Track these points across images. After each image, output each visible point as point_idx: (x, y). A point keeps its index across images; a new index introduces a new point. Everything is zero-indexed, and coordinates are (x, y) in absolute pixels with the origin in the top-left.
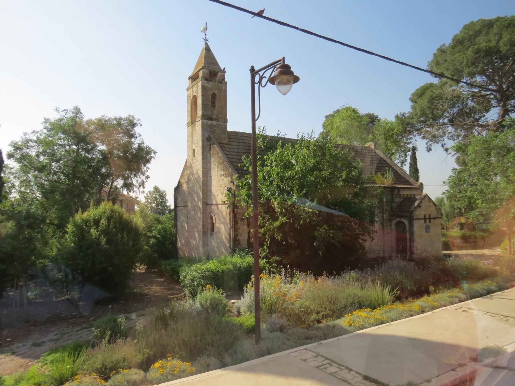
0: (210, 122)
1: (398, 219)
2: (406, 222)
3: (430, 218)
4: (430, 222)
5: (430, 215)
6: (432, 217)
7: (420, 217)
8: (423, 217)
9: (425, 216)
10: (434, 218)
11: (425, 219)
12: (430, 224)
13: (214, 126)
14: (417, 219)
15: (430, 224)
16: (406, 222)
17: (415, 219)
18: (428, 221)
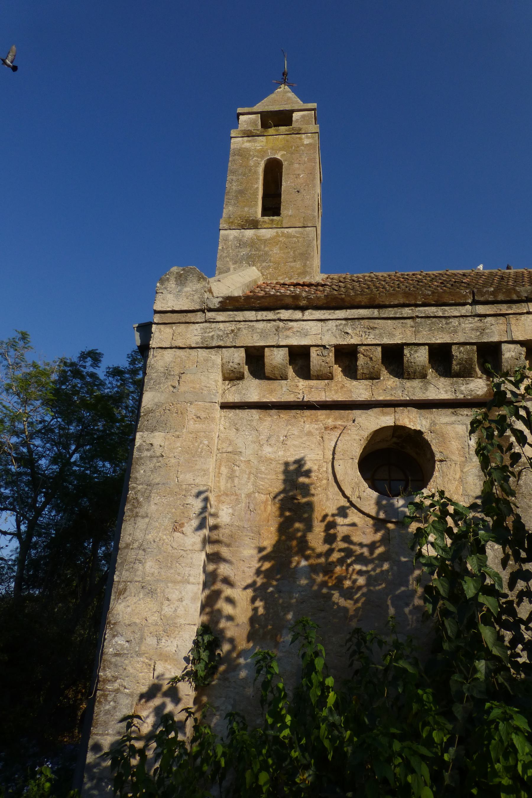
0: (249, 233)
13: (266, 240)
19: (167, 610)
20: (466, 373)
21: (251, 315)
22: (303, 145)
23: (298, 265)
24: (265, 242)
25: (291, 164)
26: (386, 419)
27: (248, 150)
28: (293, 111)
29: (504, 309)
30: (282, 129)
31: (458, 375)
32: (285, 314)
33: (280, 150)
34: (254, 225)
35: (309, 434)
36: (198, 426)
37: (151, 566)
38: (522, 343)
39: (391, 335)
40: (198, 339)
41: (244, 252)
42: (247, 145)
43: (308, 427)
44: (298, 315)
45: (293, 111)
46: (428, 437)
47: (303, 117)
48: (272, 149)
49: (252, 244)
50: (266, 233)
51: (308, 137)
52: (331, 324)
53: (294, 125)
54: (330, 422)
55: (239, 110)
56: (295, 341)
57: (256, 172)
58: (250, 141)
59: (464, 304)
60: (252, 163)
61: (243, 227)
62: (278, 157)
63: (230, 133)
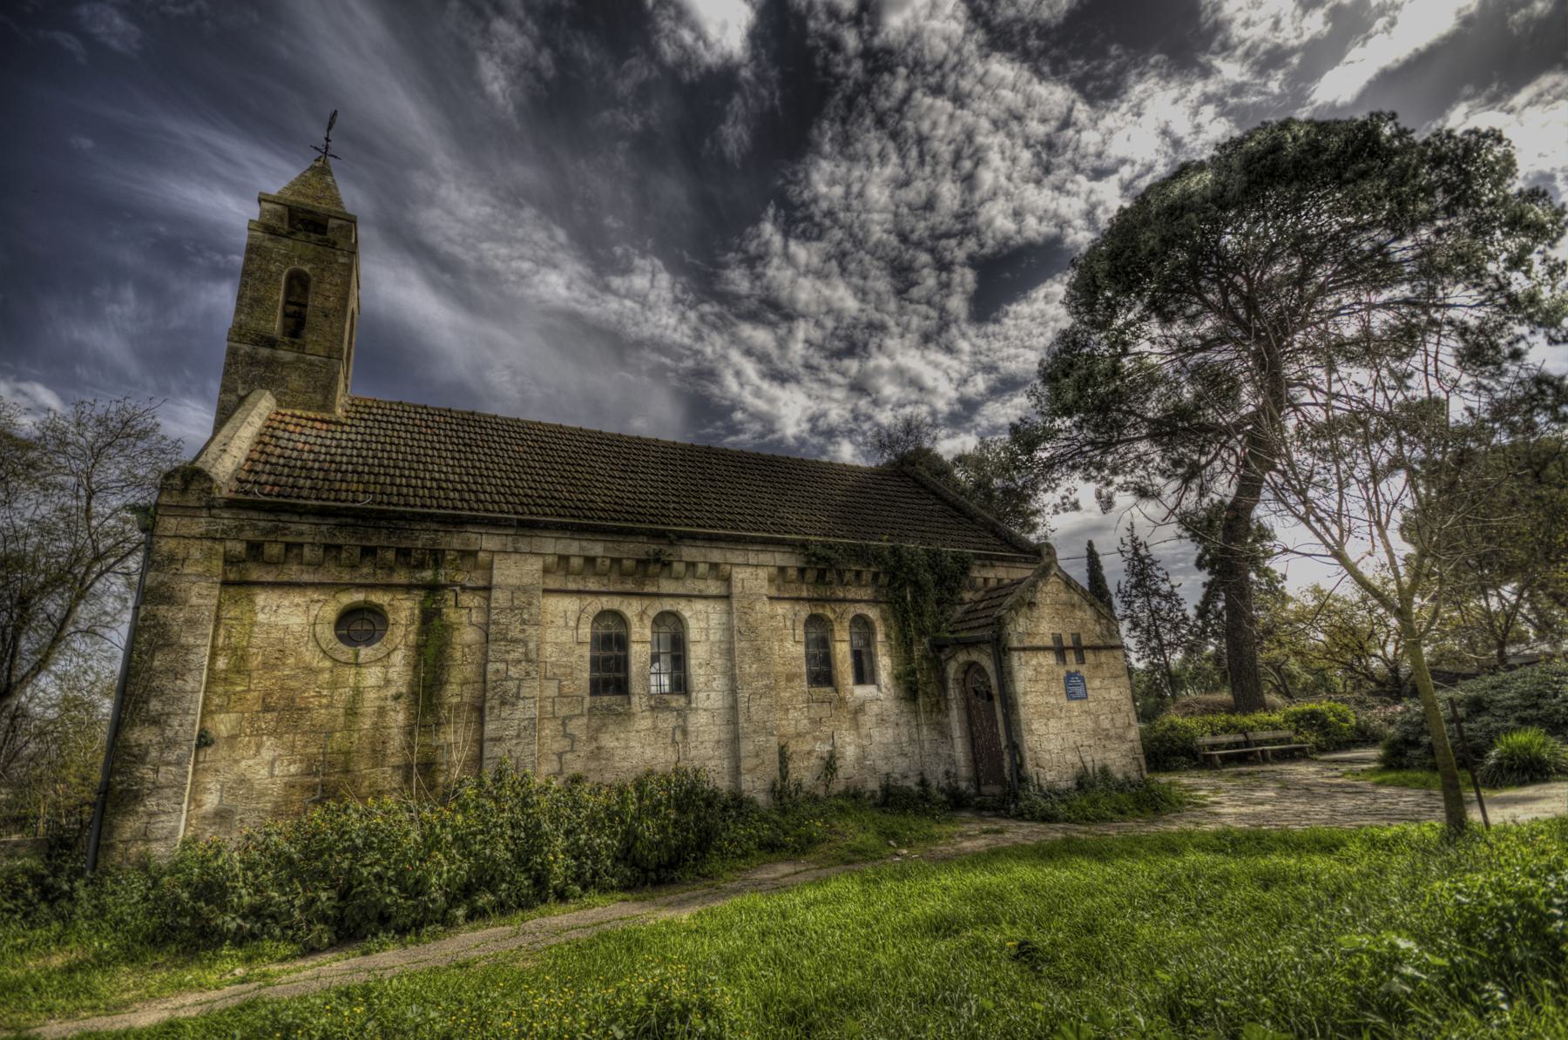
0: (264, 352)
1: (962, 657)
2: (987, 663)
3: (1079, 649)
4: (1081, 660)
5: (1077, 638)
6: (1084, 642)
7: (1037, 642)
8: (1049, 642)
9: (1058, 639)
10: (1095, 649)
11: (1060, 651)
12: (1083, 670)
14: (1024, 649)
15: (1083, 670)
16: (987, 663)
17: (1016, 649)
18: (1071, 657)
19: (169, 733)
20: (421, 566)
21: (254, 515)
24: (283, 365)
25: (320, 282)
26: (359, 597)
27: (270, 251)
30: (313, 236)
31: (415, 567)
32: (285, 517)
33: (309, 261)
34: (271, 343)
35: (298, 605)
36: (201, 601)
37: (155, 705)
39: (369, 540)
40: (203, 530)
41: (256, 371)
42: (269, 244)
43: (298, 600)
44: (296, 518)
46: (387, 608)
48: (300, 258)
49: (270, 363)
50: (286, 355)
52: (324, 528)
53: (330, 235)
54: (316, 597)
56: (289, 539)
57: (277, 281)
61: (256, 343)
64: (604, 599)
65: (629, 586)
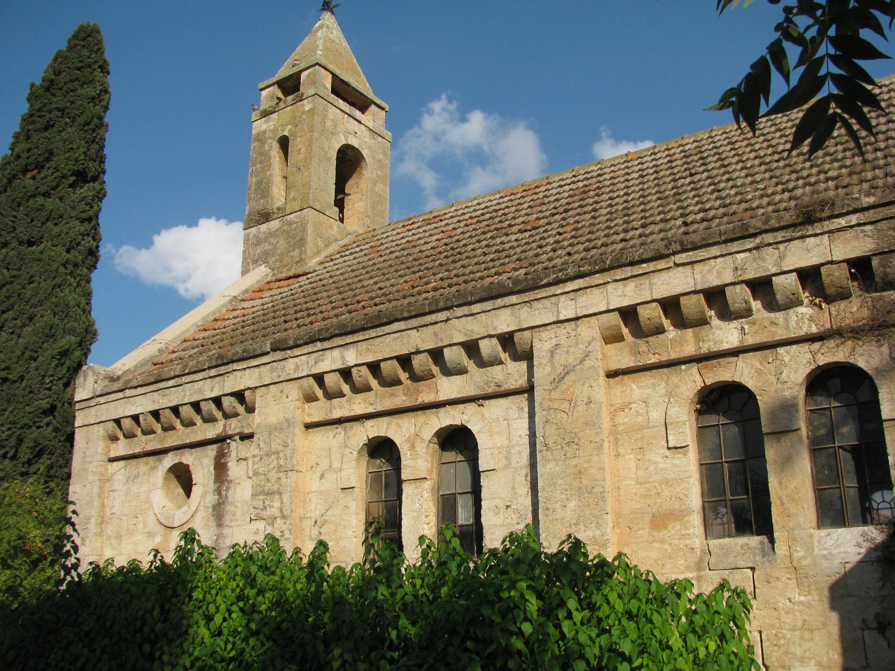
0: (263, 227)
22: (304, 112)
23: (296, 253)
25: (295, 137)
28: (301, 72)
29: (222, 370)
38: (232, 394)
45: (301, 72)
47: (309, 75)
51: (308, 103)
55: (261, 86)
58: (265, 122)
59: (204, 370)
60: (267, 147)
61: (259, 223)
62: (286, 133)
63: (251, 117)
64: (369, 424)
65: (399, 398)
